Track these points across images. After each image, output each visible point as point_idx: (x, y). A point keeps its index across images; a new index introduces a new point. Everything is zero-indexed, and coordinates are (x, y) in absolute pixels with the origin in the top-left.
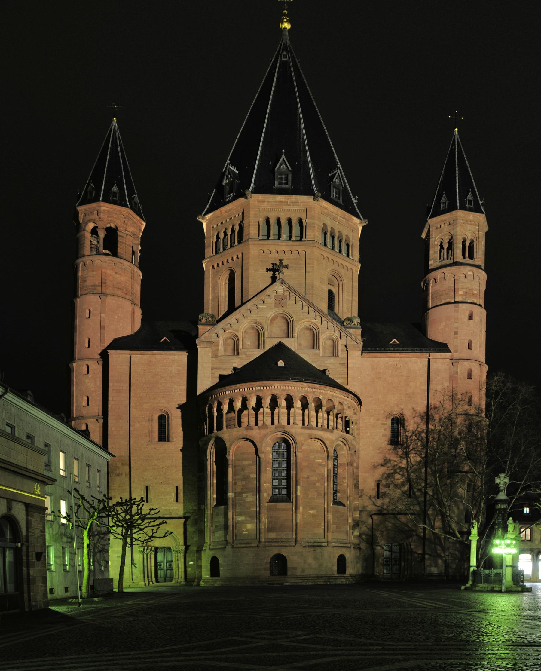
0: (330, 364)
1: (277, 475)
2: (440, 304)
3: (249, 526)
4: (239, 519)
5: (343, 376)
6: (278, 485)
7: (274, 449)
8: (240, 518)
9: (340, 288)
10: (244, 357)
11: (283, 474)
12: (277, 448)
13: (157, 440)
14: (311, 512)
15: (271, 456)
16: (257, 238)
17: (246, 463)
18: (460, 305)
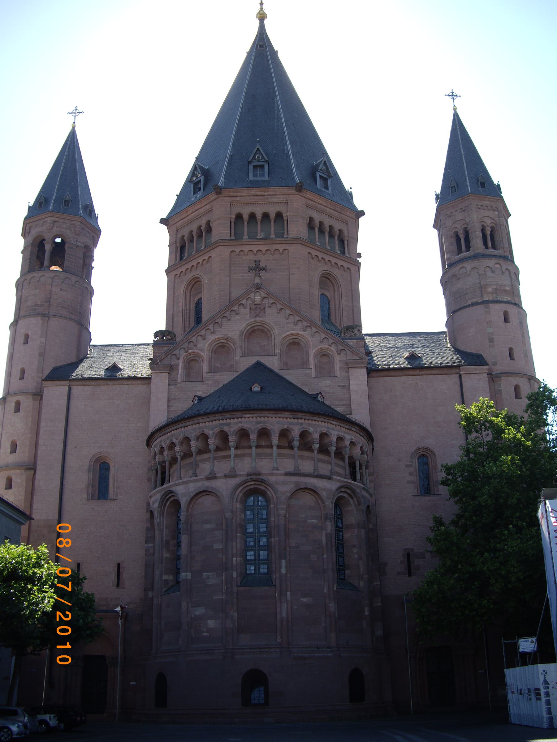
0: (326, 386)
1: (252, 544)
2: (466, 305)
3: (211, 623)
4: (198, 613)
5: (344, 402)
6: (255, 559)
7: (248, 506)
8: (199, 611)
9: (336, 292)
10: (210, 382)
11: (261, 543)
12: (251, 504)
13: (97, 498)
14: (304, 600)
15: (243, 515)
16: (229, 238)
17: (208, 526)
18: (491, 305)
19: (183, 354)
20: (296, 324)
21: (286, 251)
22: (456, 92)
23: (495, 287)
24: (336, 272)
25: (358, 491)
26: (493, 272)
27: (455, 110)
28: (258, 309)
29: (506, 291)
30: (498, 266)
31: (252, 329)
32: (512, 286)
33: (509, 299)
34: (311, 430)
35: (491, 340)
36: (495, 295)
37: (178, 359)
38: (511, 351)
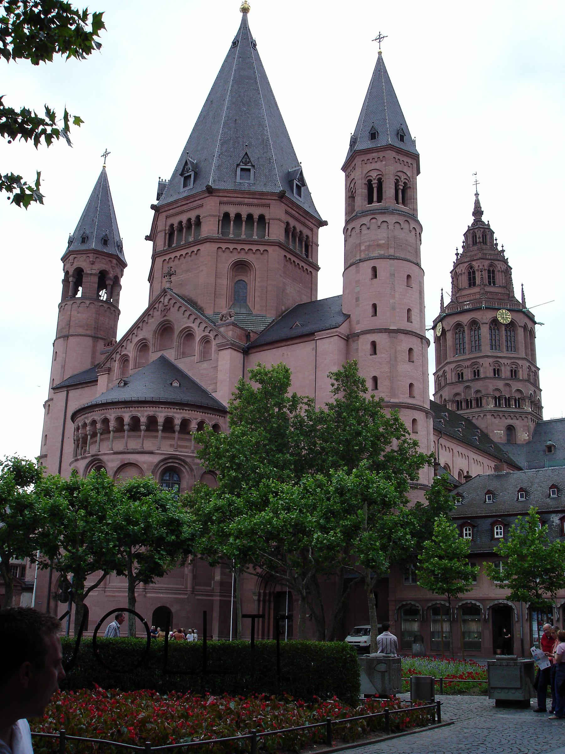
0: (204, 369)
19: (118, 356)
20: (188, 318)
21: (199, 252)
22: (376, 35)
23: (368, 244)
24: (250, 258)
25: (188, 460)
26: (368, 228)
27: (380, 53)
28: (166, 309)
29: (379, 246)
30: (374, 221)
31: (164, 327)
32: (388, 238)
33: (382, 252)
34: (139, 415)
35: (357, 299)
36: (366, 252)
37: (115, 361)
38: (375, 306)
